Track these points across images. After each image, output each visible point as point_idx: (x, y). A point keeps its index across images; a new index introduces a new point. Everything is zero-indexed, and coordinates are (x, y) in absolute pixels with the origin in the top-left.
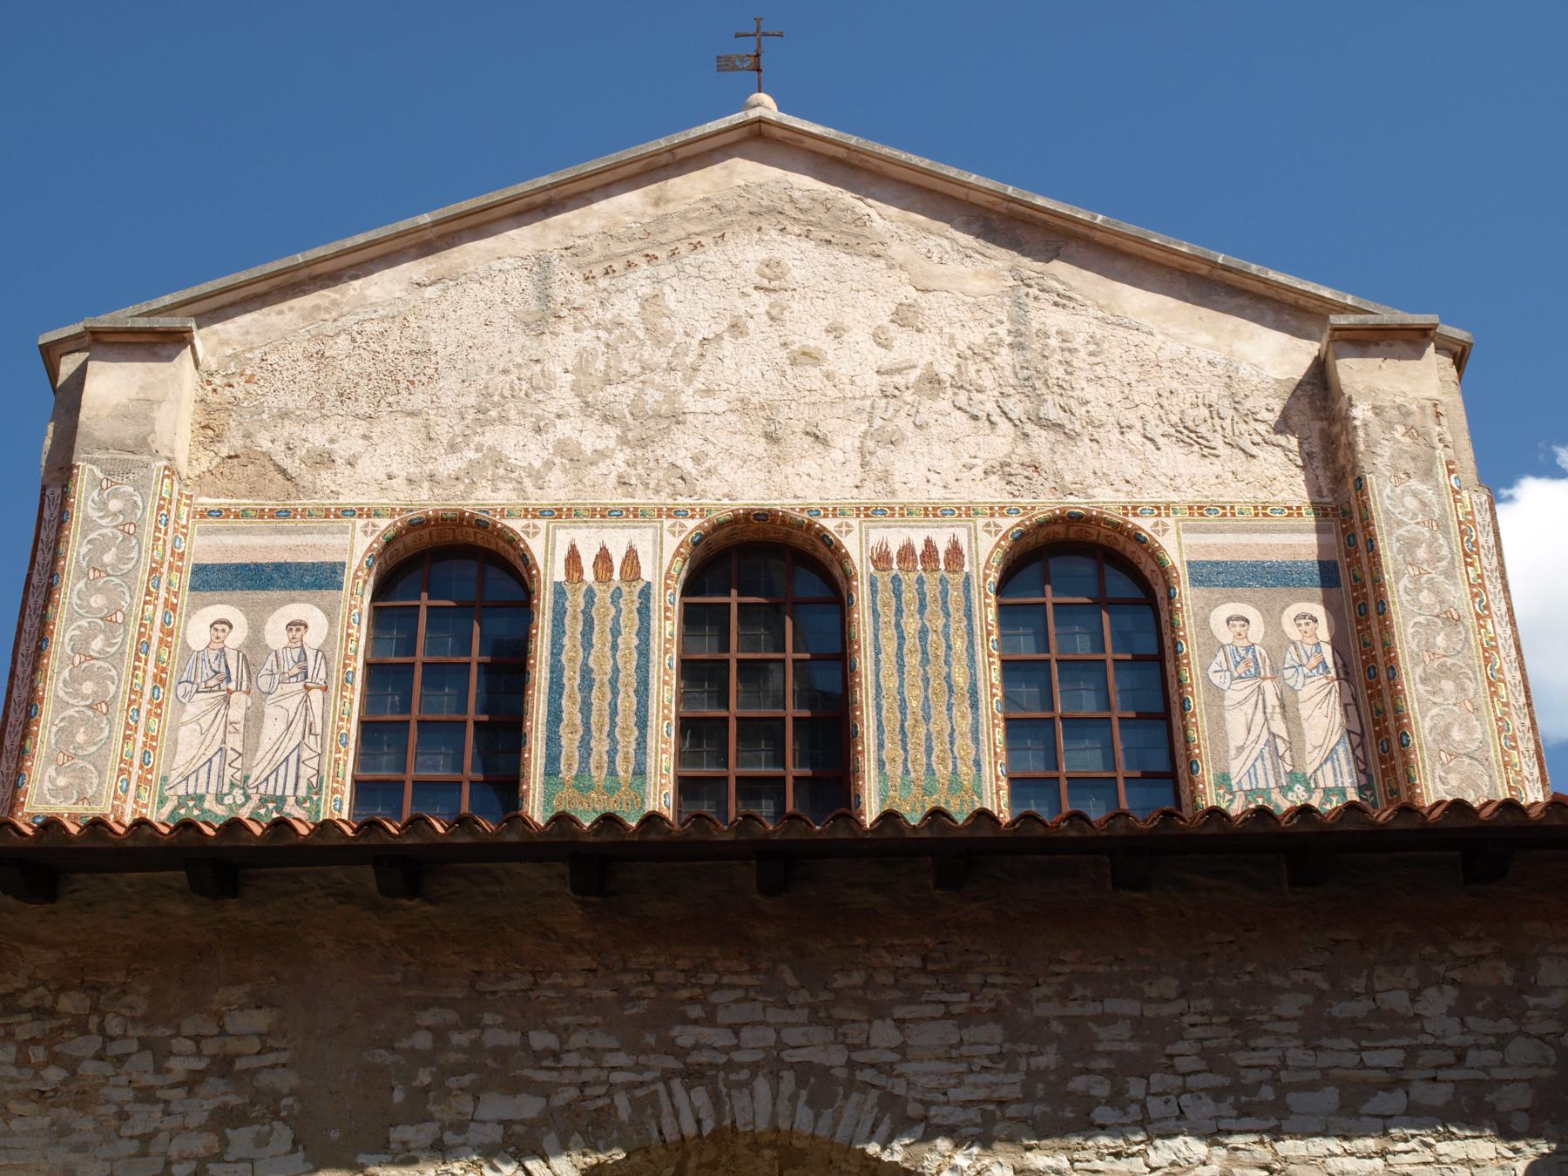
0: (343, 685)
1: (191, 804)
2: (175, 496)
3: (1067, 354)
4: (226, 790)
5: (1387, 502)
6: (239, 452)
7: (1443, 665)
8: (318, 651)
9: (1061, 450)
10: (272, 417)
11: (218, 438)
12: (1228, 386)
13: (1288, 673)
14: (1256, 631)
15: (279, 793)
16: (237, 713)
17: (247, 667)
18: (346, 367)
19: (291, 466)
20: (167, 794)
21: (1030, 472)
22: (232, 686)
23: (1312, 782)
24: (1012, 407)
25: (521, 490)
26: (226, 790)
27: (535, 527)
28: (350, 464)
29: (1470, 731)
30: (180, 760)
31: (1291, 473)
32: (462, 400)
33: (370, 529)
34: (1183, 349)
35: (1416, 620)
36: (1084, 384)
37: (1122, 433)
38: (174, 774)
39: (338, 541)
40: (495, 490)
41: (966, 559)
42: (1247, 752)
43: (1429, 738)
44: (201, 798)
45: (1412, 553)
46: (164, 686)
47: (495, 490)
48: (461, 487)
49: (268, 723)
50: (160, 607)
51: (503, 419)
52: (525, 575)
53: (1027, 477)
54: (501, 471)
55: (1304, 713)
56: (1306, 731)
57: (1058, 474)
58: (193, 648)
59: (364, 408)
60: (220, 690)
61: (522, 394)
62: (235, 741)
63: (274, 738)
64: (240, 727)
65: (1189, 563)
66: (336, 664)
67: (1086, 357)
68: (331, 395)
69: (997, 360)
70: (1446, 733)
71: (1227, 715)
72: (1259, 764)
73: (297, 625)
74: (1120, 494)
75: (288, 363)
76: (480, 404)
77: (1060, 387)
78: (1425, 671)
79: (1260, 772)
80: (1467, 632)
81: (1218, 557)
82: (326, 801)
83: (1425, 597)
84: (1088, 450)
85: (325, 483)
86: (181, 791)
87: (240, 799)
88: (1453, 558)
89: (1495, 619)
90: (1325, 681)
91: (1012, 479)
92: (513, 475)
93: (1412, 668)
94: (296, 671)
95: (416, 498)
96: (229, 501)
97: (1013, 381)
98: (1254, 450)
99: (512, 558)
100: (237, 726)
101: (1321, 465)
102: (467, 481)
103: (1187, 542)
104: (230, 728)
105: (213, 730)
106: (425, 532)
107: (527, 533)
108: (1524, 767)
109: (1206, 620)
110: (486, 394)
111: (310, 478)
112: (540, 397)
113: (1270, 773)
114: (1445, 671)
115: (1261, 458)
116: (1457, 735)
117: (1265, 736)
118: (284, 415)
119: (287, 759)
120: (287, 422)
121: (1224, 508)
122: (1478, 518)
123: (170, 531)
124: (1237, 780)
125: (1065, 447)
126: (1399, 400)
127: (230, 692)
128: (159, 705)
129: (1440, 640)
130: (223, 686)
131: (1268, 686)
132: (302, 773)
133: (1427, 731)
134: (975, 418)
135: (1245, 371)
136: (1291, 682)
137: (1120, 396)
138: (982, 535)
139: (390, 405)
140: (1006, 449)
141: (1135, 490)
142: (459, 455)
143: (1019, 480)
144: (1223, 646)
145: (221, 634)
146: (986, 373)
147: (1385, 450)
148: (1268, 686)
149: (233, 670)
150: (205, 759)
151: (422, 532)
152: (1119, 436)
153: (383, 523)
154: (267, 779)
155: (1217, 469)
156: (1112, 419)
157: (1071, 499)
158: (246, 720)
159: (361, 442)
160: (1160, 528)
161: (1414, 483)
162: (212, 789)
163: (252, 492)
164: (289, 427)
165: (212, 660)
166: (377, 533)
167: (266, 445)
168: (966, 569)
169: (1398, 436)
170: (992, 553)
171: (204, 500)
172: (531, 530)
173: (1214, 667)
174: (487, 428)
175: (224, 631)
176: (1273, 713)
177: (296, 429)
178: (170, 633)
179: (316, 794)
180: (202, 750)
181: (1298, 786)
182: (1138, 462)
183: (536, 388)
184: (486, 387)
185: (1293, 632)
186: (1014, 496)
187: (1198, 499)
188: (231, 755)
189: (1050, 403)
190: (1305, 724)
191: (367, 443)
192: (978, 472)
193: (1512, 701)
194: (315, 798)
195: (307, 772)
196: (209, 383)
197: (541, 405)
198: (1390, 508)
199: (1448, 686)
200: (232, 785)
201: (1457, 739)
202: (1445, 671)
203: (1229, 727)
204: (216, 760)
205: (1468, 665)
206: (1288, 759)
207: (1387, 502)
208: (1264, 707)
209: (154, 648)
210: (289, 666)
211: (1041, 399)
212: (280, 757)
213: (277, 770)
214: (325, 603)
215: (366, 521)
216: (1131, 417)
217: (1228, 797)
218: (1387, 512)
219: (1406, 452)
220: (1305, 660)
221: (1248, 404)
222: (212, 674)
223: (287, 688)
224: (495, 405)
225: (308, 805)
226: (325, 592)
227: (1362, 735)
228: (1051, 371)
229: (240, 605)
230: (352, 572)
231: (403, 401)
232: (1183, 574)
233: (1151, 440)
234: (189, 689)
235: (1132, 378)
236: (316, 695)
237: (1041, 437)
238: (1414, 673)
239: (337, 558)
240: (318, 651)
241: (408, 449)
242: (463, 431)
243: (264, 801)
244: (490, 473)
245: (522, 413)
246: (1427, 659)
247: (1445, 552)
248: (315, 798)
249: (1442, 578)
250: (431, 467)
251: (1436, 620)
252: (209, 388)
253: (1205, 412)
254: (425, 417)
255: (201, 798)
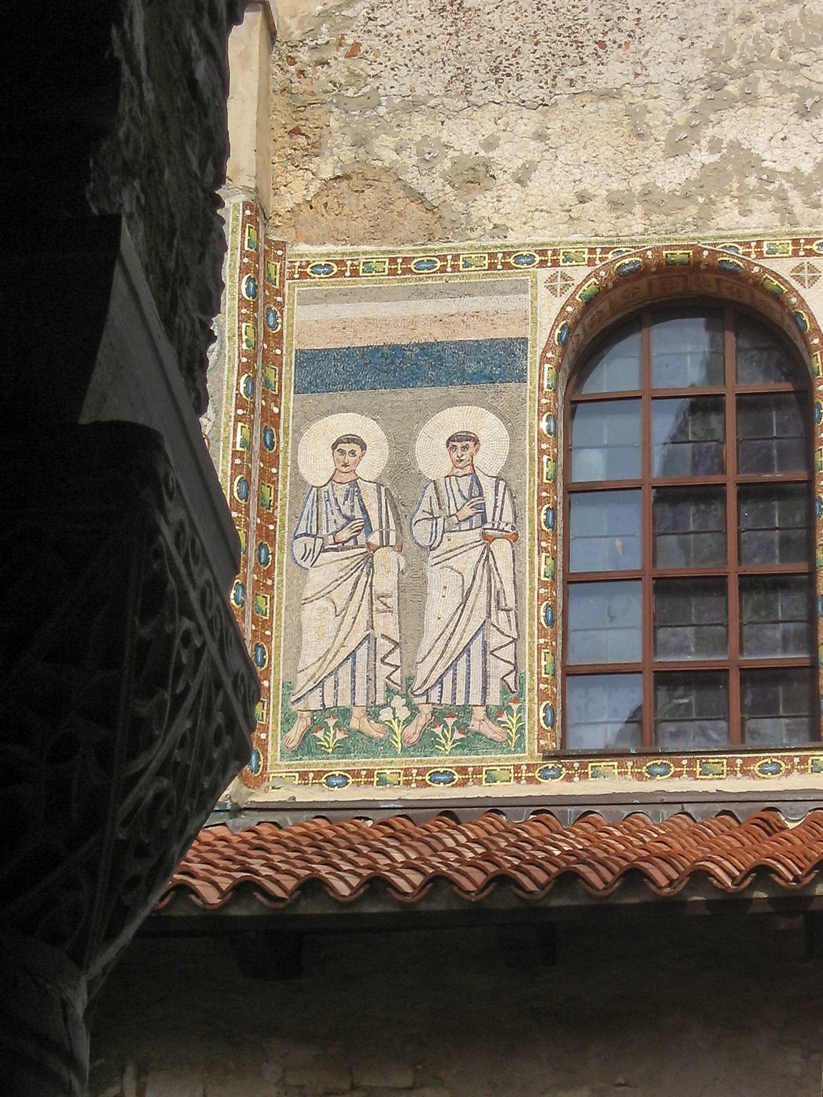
0: (541, 531)
1: (331, 722)
2: (263, 246)
4: (380, 700)
6: (348, 171)
8: (498, 479)
10: (393, 110)
11: (315, 150)
15: (460, 701)
16: (385, 581)
17: (395, 507)
18: (498, 25)
19: (432, 187)
20: (294, 708)
22: (375, 539)
25: (786, 212)
26: (380, 701)
27: (812, 269)
28: (519, 181)
30: (309, 657)
32: (682, 69)
33: (559, 283)
38: (302, 679)
39: (512, 303)
40: (744, 213)
44: (345, 713)
46: (273, 545)
47: (744, 213)
48: (693, 210)
49: (434, 593)
50: (258, 422)
51: (750, 98)
52: (801, 345)
54: (752, 181)
58: (311, 483)
59: (531, 91)
60: (356, 545)
61: (774, 54)
62: (387, 624)
63: (446, 618)
64: (392, 602)
66: (529, 497)
68: (480, 71)
73: (463, 441)
75: (408, 21)
76: (709, 74)
82: (531, 710)
85: (484, 213)
86: (314, 703)
87: (404, 713)
92: (771, 187)
94: (468, 511)
95: (626, 231)
96: (340, 248)
99: (777, 317)
100: (388, 601)
102: (701, 200)
104: (378, 605)
105: (353, 608)
106: (642, 284)
107: (800, 280)
110: (716, 56)
111: (460, 206)
112: (802, 58)
118: (413, 105)
119: (467, 649)
120: (417, 118)
123: (260, 303)
127: (372, 548)
128: (269, 574)
130: (361, 538)
132: (491, 670)
139: (572, 82)
142: (684, 158)
145: (349, 459)
149: (374, 515)
150: (344, 653)
151: (637, 284)
153: (579, 273)
154: (440, 681)
158: (401, 588)
159: (533, 144)
162: (361, 699)
163: (376, 232)
164: (420, 126)
165: (341, 500)
166: (572, 289)
167: (389, 156)
171: (303, 248)
172: (806, 274)
174: (726, 113)
175: (353, 453)
177: (430, 129)
178: (274, 462)
179: (516, 701)
180: (337, 644)
183: (793, 44)
184: (717, 47)
188: (385, 647)
191: (542, 146)
194: (515, 707)
195: (499, 668)
196: (292, 61)
197: (804, 71)
200: (388, 690)
204: (362, 653)
209: (254, 487)
210: (455, 502)
212: (456, 645)
213: (453, 666)
214: (501, 404)
215: (552, 271)
222: (342, 521)
223: (458, 539)
224: (733, 75)
225: (504, 718)
226: (501, 386)
229: (373, 413)
230: (539, 352)
231: (590, 77)
234: (310, 546)
236: (502, 549)
239: (513, 332)
240: (498, 479)
241: (606, 152)
242: (689, 120)
243: (438, 716)
244: (735, 185)
245: (776, 85)
248: (515, 707)
250: (644, 180)
252: (292, 69)
254: (629, 99)
255: (345, 713)
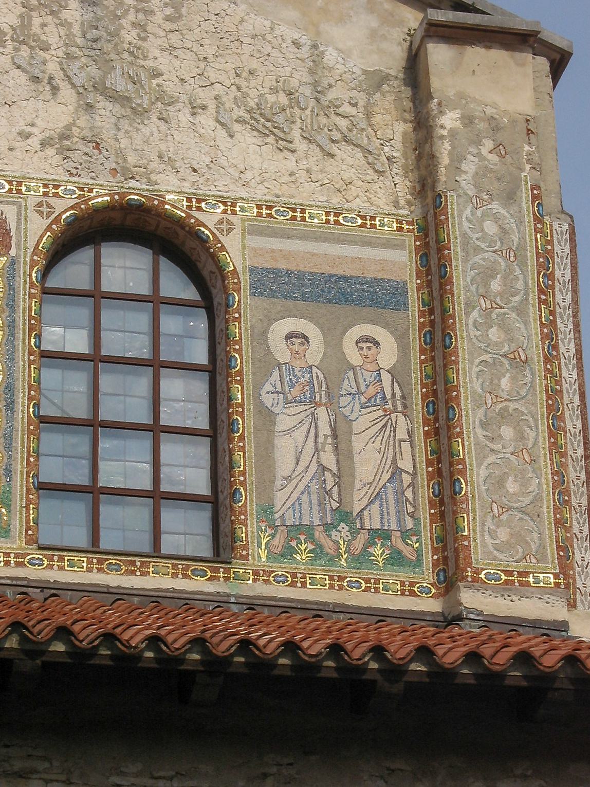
3: (141, 16)
5: (466, 225)
7: (506, 409)
9: (126, 127)
12: (312, 72)
13: (344, 401)
14: (315, 351)
21: (89, 149)
23: (358, 521)
24: (76, 71)
29: (525, 483)
31: (368, 178)
34: (267, 24)
35: (482, 358)
36: (157, 53)
37: (194, 114)
41: (13, 243)
42: (294, 482)
43: (484, 488)
45: (486, 285)
53: (87, 154)
55: (357, 443)
56: (357, 465)
57: (119, 153)
65: (253, 270)
67: (161, 21)
69: (65, 15)
70: (500, 483)
71: (276, 442)
72: (305, 498)
74: (186, 184)
77: (131, 53)
78: (486, 415)
79: (305, 506)
80: (533, 374)
81: (283, 265)
83: (494, 334)
84: (155, 130)
88: (527, 294)
89: (563, 360)
90: (381, 413)
91: (69, 154)
93: (473, 409)
97: (79, 41)
98: (334, 149)
101: (400, 172)
103: (253, 245)
108: (575, 523)
109: (264, 333)
113: (316, 508)
114: (504, 415)
115: (338, 158)
116: (512, 486)
117: (314, 467)
121: (294, 210)
122: (557, 249)
124: (280, 513)
125: (131, 125)
126: (489, 111)
129: (505, 382)
131: (322, 413)
133: (481, 480)
134: (36, 79)
135: (331, 56)
136: (346, 411)
137: (195, 71)
138: (33, 216)
140: (66, 120)
141: (202, 180)
143: (76, 156)
144: (279, 365)
146: (51, 28)
147: (470, 166)
148: (322, 413)
152: (188, 116)
155: (291, 164)
156: (184, 98)
157: (132, 183)
160: (224, 226)
161: (495, 206)
168: (13, 252)
169: (484, 151)
170: (42, 237)
173: (268, 387)
176: (324, 444)
181: (342, 525)
182: (207, 149)
185: (354, 356)
186: (71, 175)
187: (268, 198)
189: (118, 71)
190: (356, 459)
192: (34, 142)
193: (570, 452)
198: (469, 231)
199: (507, 432)
201: (511, 490)
202: (504, 415)
203: (277, 455)
205: (530, 412)
206: (335, 496)
207: (466, 225)
208: (316, 436)
211: (106, 65)
216: (205, 96)
217: (269, 531)
218: (464, 235)
219: (491, 171)
220: (363, 389)
221: (331, 95)
227: (414, 475)
228: (123, 32)
232: (245, 280)
233: (222, 124)
235: (210, 51)
237: (106, 110)
238: (474, 416)
246: (489, 401)
247: (520, 285)
249: (514, 315)
251: (503, 359)
253: (283, 99)
